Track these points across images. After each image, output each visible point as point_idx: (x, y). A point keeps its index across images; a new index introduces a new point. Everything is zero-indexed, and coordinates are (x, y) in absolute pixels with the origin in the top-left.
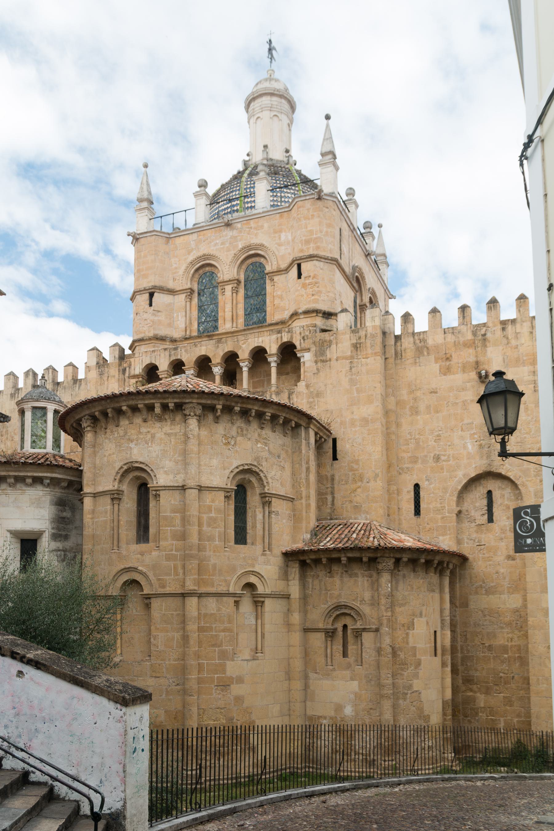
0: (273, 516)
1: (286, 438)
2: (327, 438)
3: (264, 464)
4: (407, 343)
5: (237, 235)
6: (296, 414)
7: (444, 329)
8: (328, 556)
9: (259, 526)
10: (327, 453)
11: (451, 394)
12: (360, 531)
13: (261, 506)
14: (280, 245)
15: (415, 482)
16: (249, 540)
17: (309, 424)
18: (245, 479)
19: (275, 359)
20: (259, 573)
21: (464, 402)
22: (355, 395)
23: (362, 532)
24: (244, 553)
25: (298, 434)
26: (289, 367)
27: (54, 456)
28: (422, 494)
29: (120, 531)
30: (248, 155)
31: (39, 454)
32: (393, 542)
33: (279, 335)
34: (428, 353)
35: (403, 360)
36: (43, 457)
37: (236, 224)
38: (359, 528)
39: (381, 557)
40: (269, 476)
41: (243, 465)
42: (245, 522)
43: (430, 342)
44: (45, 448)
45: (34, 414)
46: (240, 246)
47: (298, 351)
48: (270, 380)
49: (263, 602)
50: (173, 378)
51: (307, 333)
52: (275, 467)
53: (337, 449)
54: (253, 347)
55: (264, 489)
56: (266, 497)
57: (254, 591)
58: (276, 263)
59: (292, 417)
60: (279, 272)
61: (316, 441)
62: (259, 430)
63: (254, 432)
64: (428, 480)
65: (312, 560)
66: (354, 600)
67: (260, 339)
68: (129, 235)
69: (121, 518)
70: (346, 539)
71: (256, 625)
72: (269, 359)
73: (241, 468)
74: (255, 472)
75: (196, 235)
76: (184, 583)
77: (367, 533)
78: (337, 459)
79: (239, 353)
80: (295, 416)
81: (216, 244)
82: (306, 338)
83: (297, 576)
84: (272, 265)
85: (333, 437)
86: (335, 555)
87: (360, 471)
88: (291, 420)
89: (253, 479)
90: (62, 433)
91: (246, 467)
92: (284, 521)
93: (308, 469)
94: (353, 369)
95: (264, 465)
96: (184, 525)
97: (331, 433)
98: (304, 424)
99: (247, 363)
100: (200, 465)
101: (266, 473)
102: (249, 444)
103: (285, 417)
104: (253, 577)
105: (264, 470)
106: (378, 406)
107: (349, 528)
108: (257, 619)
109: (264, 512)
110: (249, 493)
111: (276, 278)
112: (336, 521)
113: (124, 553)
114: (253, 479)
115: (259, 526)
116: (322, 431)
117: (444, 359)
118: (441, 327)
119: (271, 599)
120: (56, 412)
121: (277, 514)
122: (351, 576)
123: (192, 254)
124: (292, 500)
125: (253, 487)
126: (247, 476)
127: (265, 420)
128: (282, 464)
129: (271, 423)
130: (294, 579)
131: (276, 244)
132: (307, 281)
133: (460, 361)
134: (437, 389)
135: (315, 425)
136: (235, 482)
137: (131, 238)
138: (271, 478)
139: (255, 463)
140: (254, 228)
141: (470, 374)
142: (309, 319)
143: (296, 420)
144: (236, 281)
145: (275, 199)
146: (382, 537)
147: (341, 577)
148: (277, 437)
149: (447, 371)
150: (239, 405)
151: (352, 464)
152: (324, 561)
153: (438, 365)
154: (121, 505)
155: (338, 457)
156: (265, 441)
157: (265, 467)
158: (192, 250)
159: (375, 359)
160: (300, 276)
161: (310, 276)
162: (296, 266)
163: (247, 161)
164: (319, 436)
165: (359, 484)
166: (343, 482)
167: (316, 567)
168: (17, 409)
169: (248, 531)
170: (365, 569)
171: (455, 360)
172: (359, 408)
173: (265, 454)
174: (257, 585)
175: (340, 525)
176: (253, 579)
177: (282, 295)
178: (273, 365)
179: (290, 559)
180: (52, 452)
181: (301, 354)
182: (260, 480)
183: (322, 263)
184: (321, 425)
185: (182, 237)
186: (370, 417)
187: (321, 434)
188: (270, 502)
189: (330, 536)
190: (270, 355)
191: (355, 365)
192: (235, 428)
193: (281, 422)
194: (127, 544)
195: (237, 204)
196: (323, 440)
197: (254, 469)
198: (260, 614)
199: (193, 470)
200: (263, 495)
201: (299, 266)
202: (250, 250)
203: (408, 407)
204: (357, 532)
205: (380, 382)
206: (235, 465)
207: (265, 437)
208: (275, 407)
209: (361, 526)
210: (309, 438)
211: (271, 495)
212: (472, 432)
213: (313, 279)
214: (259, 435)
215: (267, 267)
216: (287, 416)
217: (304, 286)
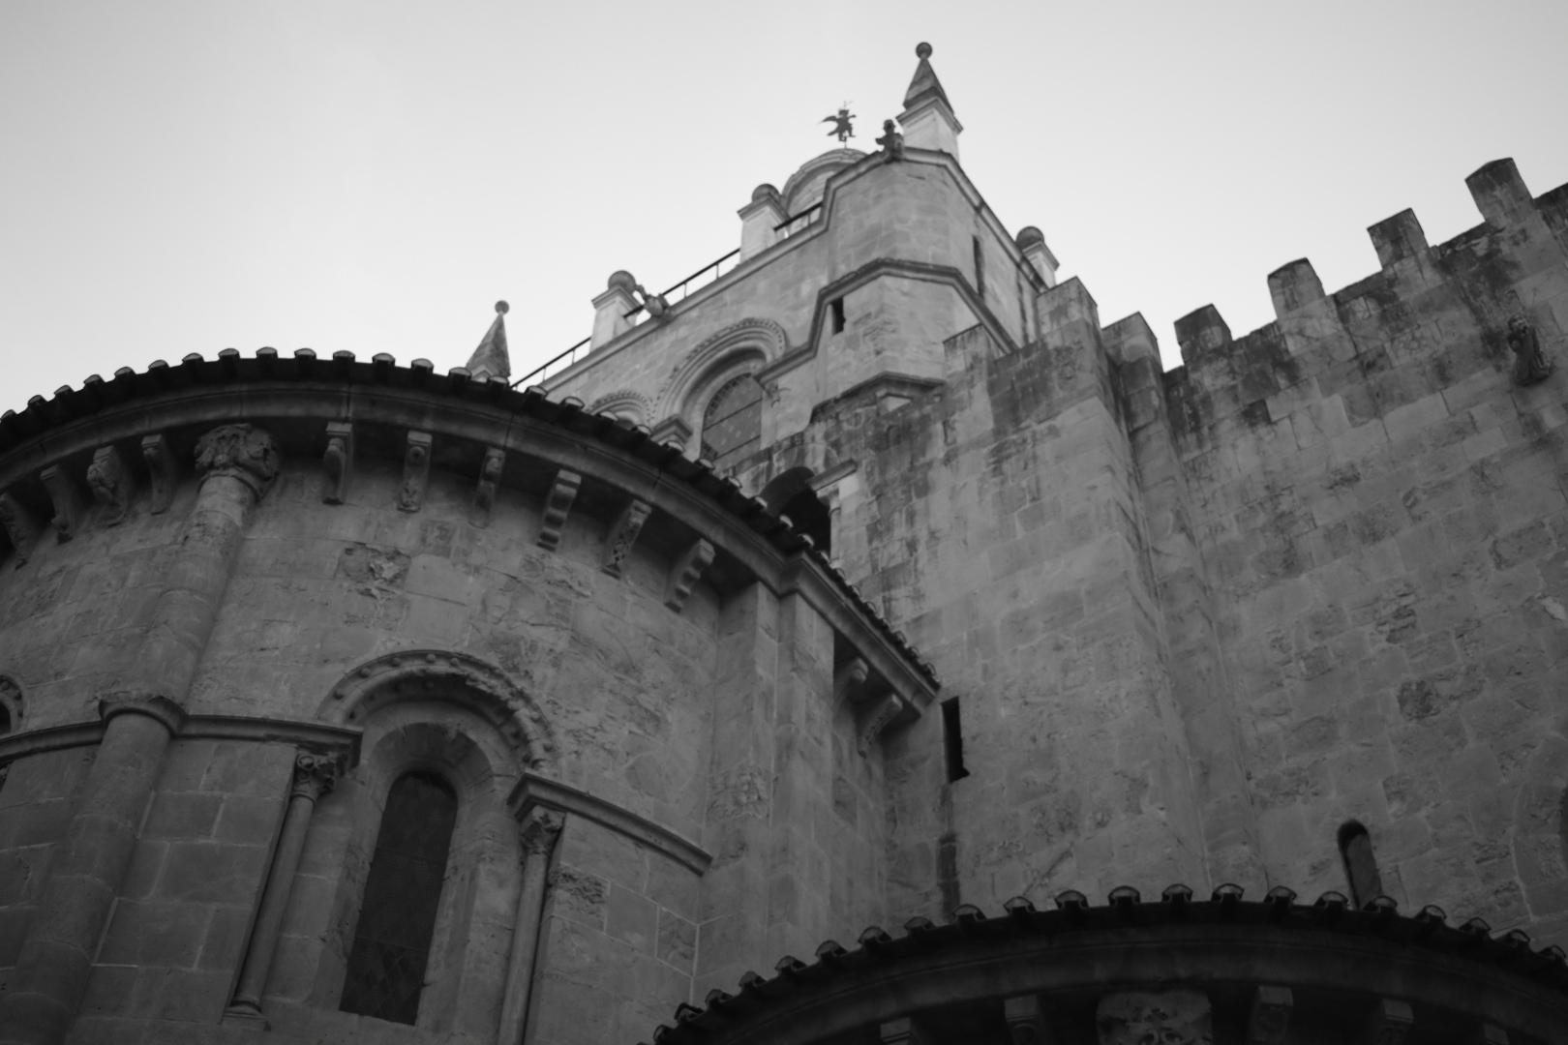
0: (561, 894)
1: (681, 622)
2: (917, 704)
3: (542, 671)
4: (1210, 379)
7: (1335, 296)
10: (924, 760)
11: (1416, 463)
13: (513, 857)
16: (425, 1018)
17: (789, 573)
21: (1480, 471)
22: (1020, 532)
25: (742, 612)
34: (1294, 379)
35: (1205, 430)
37: (686, 316)
40: (561, 725)
41: (421, 655)
43: (1293, 346)
47: (821, 478)
53: (965, 734)
56: (532, 802)
59: (694, 520)
62: (535, 551)
63: (505, 549)
73: (413, 667)
74: (492, 700)
75: (586, 374)
78: (964, 773)
82: (843, 440)
85: (942, 697)
88: (696, 536)
89: (485, 740)
91: (441, 667)
94: (1006, 467)
95: (537, 675)
97: (936, 686)
101: (546, 710)
102: (473, 587)
105: (540, 697)
110: (464, 811)
114: (485, 740)
116: (874, 644)
117: (1359, 374)
118: (1321, 291)
121: (591, 892)
124: (697, 861)
125: (483, 777)
126: (455, 722)
128: (649, 700)
132: (861, 330)
133: (1423, 355)
134: (1352, 466)
138: (575, 734)
139: (493, 660)
141: (1473, 377)
144: (673, 428)
148: (630, 598)
149: (1377, 403)
150: (428, 424)
153: (1338, 400)
155: (969, 762)
156: (559, 592)
157: (543, 681)
159: (1080, 411)
160: (839, 324)
162: (830, 309)
166: (995, 855)
169: (431, 975)
171: (1403, 359)
181: (831, 488)
182: (519, 739)
183: (906, 282)
188: (558, 833)
191: (1013, 450)
192: (411, 526)
197: (484, 682)
201: (838, 307)
202: (717, 349)
207: (558, 577)
211: (559, 799)
212: (1550, 556)
213: (876, 317)
214: (530, 564)
216: (670, 506)
217: (852, 343)
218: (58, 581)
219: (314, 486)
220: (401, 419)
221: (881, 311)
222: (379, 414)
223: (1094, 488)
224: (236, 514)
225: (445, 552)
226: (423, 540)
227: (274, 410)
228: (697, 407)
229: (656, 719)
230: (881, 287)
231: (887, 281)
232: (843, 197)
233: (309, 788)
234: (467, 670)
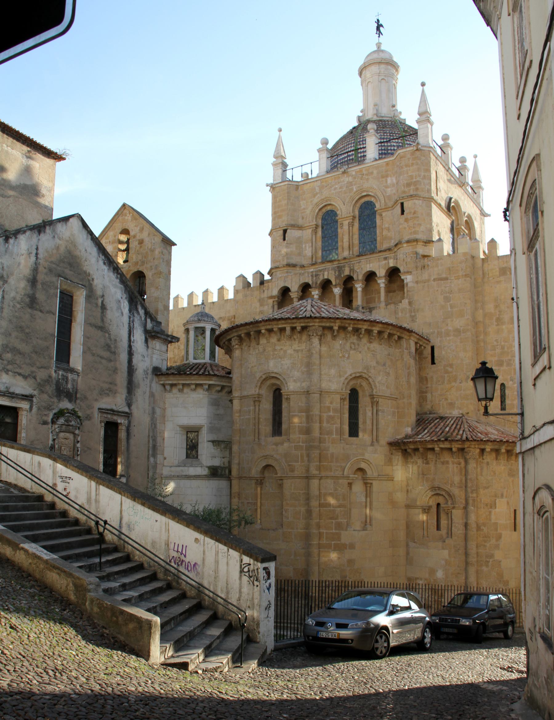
0: (380, 413)
3: (372, 371)
5: (352, 180)
6: (397, 329)
8: (425, 447)
9: (369, 422)
12: (453, 424)
13: (370, 405)
14: (387, 187)
15: (502, 382)
17: (410, 336)
18: (357, 383)
19: (383, 281)
20: (368, 460)
22: (449, 309)
23: (454, 426)
24: (356, 445)
25: (401, 345)
26: (395, 286)
27: (211, 365)
28: (507, 392)
29: (260, 427)
30: (362, 112)
31: (200, 364)
32: (479, 434)
33: (386, 261)
36: (203, 366)
38: (452, 422)
39: (468, 447)
41: (355, 373)
42: (357, 419)
44: (204, 358)
45: (195, 332)
46: (355, 190)
48: (379, 298)
49: (371, 484)
50: (301, 302)
51: (409, 260)
52: (381, 373)
54: (366, 271)
55: (372, 392)
56: (374, 398)
57: (364, 474)
58: (383, 202)
59: (395, 332)
60: (386, 209)
61: (416, 350)
62: (368, 344)
64: (511, 380)
65: (411, 449)
66: (446, 484)
67: (371, 265)
68: (267, 186)
69: (260, 416)
70: (441, 432)
71: (366, 502)
72: (379, 281)
73: (354, 376)
76: (309, 468)
77: (458, 427)
79: (355, 277)
80: (398, 331)
81: (335, 189)
83: (400, 463)
84: (380, 203)
85: (431, 344)
86: (430, 446)
87: (454, 373)
88: (394, 335)
90: (217, 348)
91: (358, 375)
92: (389, 417)
93: (409, 374)
96: (308, 422)
98: (406, 337)
99: (361, 284)
100: (321, 374)
103: (389, 333)
104: (363, 463)
106: (468, 319)
107: (444, 422)
108: (366, 497)
109: (373, 410)
111: (384, 214)
112: (435, 415)
113: (263, 444)
114: (364, 384)
115: (369, 422)
119: (377, 481)
120: (213, 331)
121: (383, 412)
122: (443, 463)
123: (316, 197)
127: (373, 336)
128: (387, 371)
129: (378, 337)
130: (397, 465)
131: (384, 186)
135: (416, 337)
136: (349, 388)
137: (269, 188)
138: (378, 382)
139: (365, 371)
140: (367, 175)
142: (410, 247)
143: (398, 334)
145: (383, 148)
146: (471, 430)
147: (436, 464)
151: (447, 368)
152: (421, 450)
154: (261, 405)
155: (436, 361)
156: (373, 353)
158: (317, 194)
160: (403, 212)
161: (411, 212)
162: (399, 205)
163: (361, 117)
164: (419, 345)
165: (453, 384)
167: (415, 455)
168: (183, 329)
170: (455, 457)
172: (452, 321)
173: (374, 364)
174: (367, 470)
175: (437, 419)
176: (363, 465)
177: (389, 227)
178: (382, 285)
179: (394, 448)
180: (209, 361)
184: (420, 336)
185: (309, 184)
186: (462, 328)
187: (421, 343)
188: (378, 402)
189: (428, 429)
190: (380, 277)
193: (386, 337)
194: (266, 436)
195: (352, 155)
196: (423, 347)
197: (364, 375)
198: (368, 495)
199: (315, 378)
200: (372, 396)
201: (402, 204)
203: (494, 318)
204: (450, 426)
205: (470, 299)
206: (349, 373)
208: (380, 325)
209: (454, 420)
210: (410, 348)
214: (368, 348)
215: (376, 205)
216: (391, 332)
217: (406, 220)
218: (282, 352)
219: (329, 337)
220: (347, 325)
221: (415, 213)
222: (343, 325)
223: (466, 303)
224: (319, 346)
225: (355, 349)
226: (351, 347)
227: (323, 324)
228: (357, 208)
229: (389, 373)
230: (415, 203)
231: (416, 201)
232: (401, 158)
233: (342, 401)
234: (362, 374)
